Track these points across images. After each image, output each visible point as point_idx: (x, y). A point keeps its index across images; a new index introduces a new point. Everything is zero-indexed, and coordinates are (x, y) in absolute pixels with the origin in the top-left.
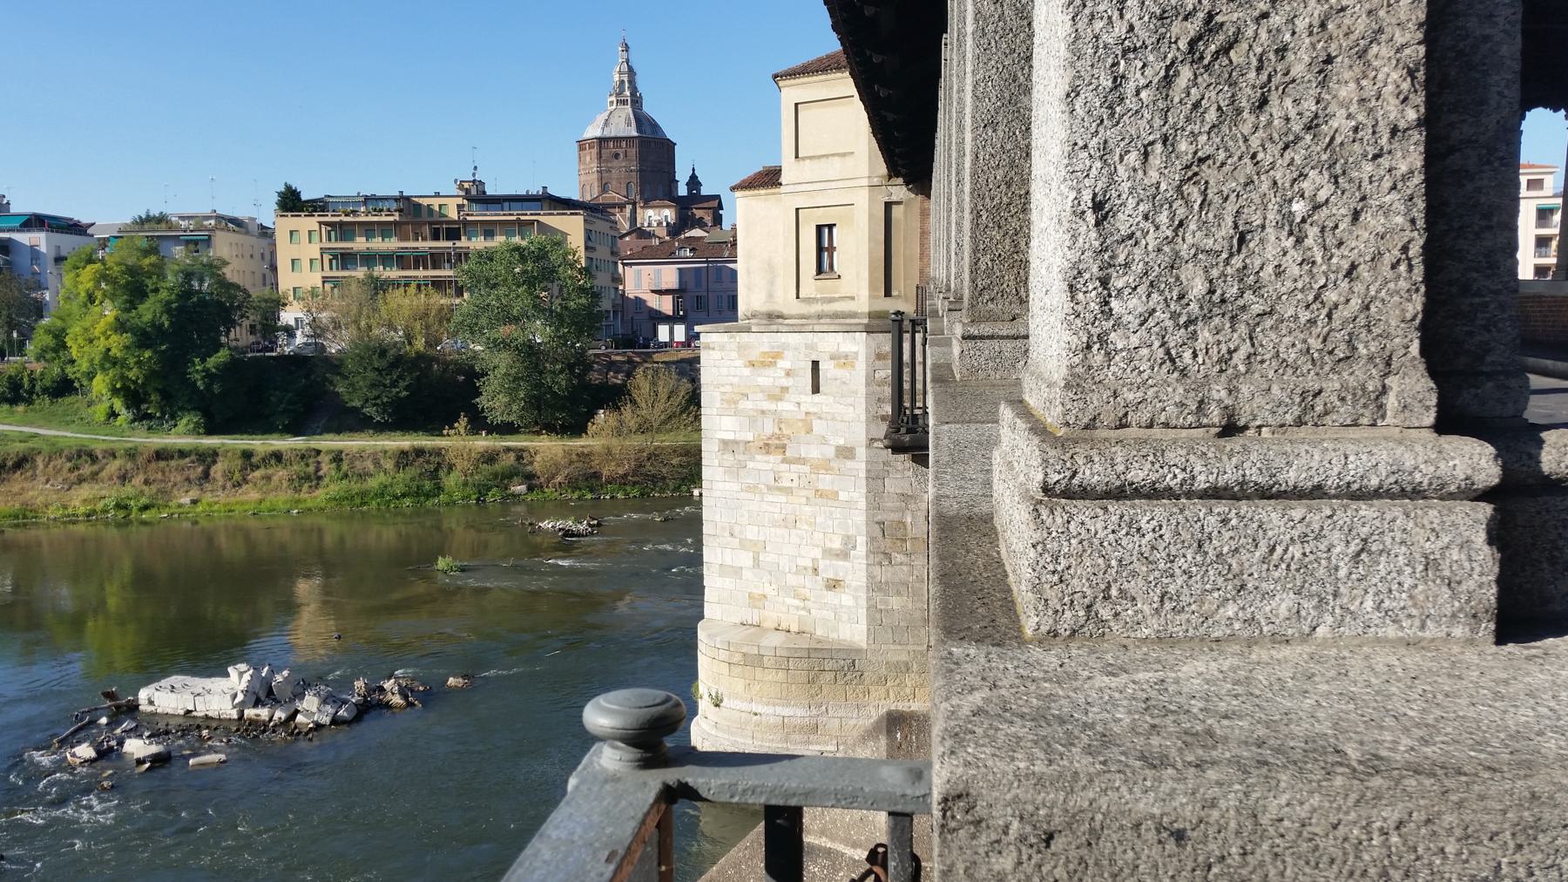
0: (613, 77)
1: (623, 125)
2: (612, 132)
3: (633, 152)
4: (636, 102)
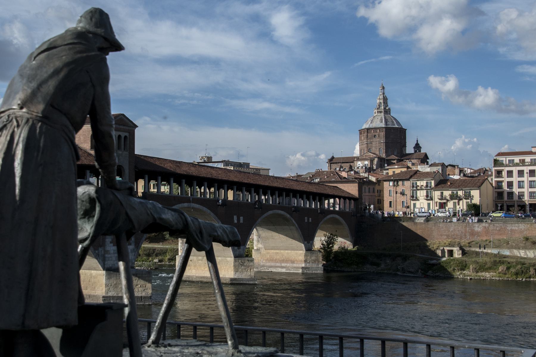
0: (377, 101)
1: (379, 122)
2: (374, 125)
3: (383, 134)
4: (387, 112)
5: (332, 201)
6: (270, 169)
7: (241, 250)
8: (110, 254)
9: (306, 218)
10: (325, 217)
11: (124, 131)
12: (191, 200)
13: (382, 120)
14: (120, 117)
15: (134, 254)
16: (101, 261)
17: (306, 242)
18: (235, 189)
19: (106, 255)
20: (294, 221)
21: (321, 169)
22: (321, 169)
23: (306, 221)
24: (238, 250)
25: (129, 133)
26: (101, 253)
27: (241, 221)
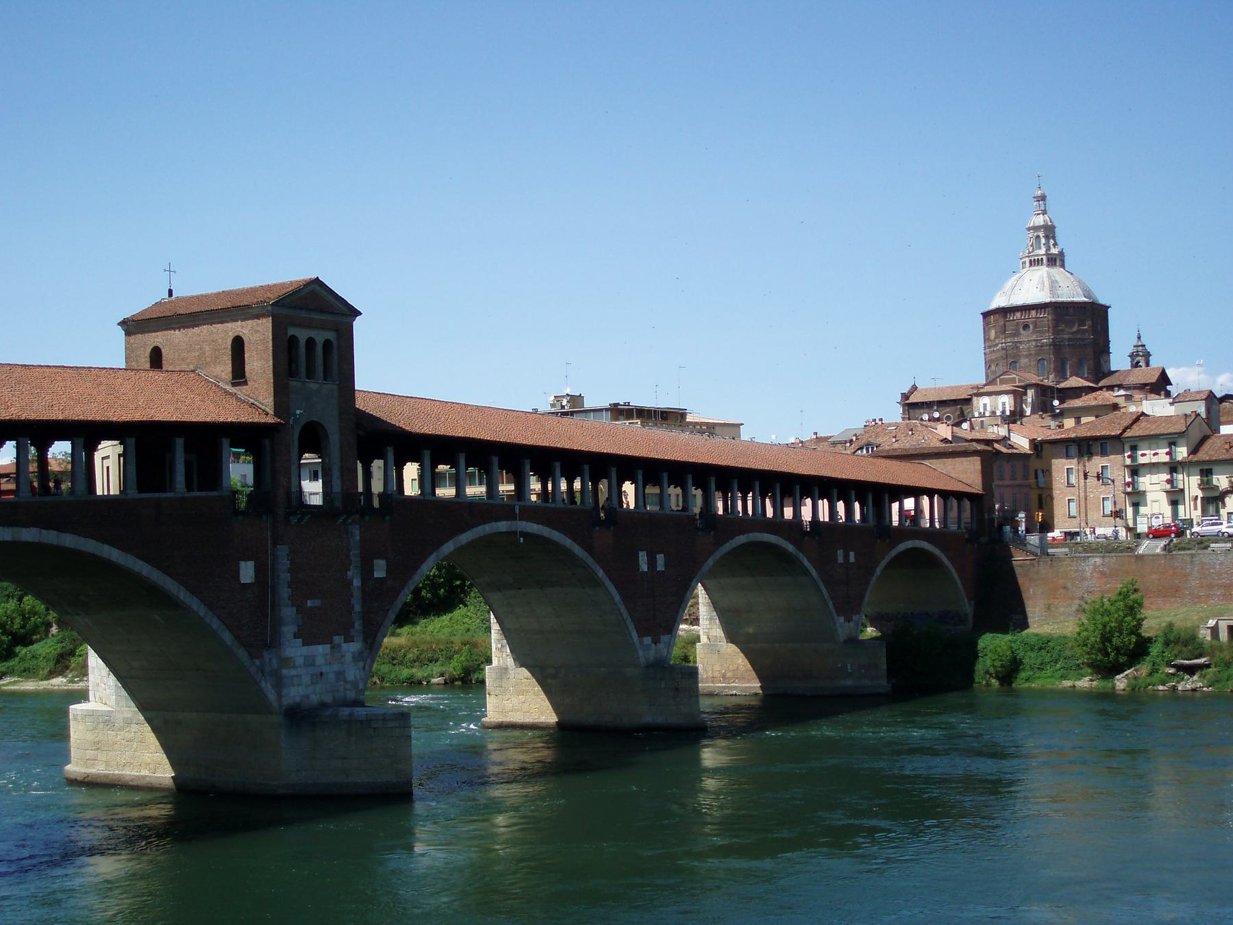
5: (909, 503)
6: (742, 424)
7: (660, 646)
8: (294, 667)
9: (840, 553)
10: (892, 547)
11: (323, 327)
12: (517, 511)
13: (1043, 283)
14: (310, 288)
15: (361, 664)
16: (270, 687)
17: (842, 619)
18: (640, 477)
19: (285, 671)
20: (806, 562)
21: (881, 420)
22: (881, 420)
23: (840, 560)
24: (653, 644)
25: (337, 331)
27: (660, 566)
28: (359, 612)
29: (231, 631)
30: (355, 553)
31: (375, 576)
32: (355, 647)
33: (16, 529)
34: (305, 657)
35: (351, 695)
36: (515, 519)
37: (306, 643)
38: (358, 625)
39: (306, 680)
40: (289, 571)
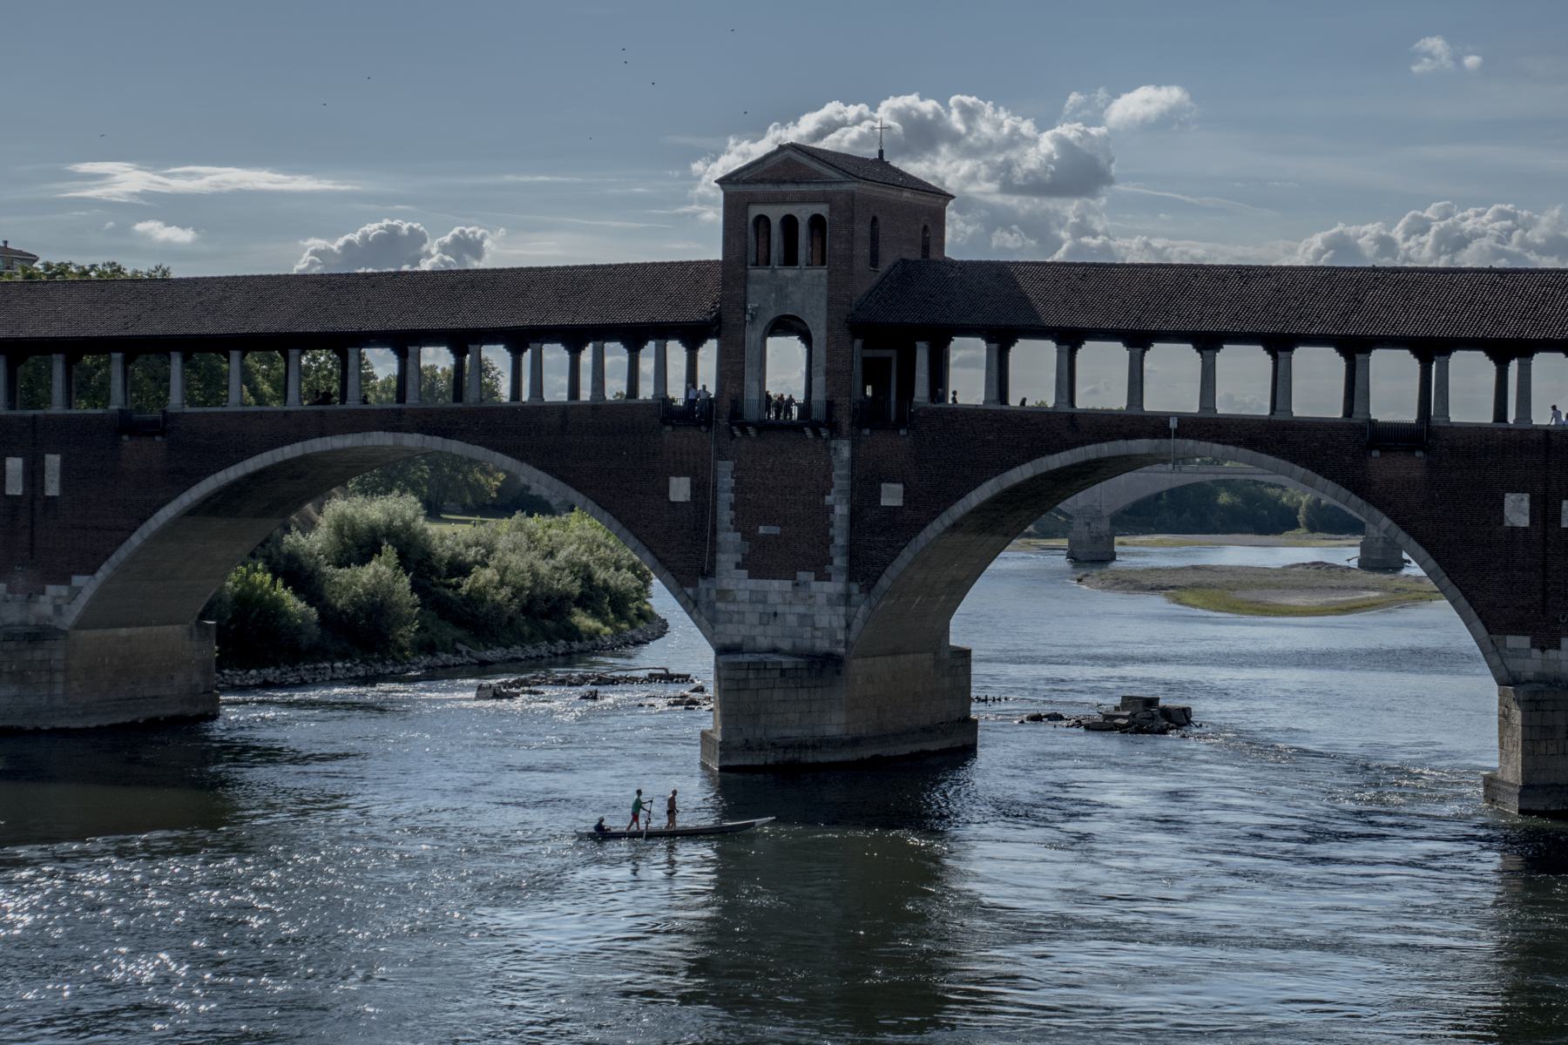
8: (734, 601)
11: (804, 199)
19: (720, 605)
24: (1536, 653)
26: (708, 595)
28: (843, 546)
29: (654, 553)
30: (840, 477)
31: (882, 504)
32: (835, 587)
33: (399, 435)
34: (751, 591)
35: (822, 645)
36: (1168, 437)
37: (750, 577)
38: (839, 561)
39: (752, 618)
40: (733, 490)
